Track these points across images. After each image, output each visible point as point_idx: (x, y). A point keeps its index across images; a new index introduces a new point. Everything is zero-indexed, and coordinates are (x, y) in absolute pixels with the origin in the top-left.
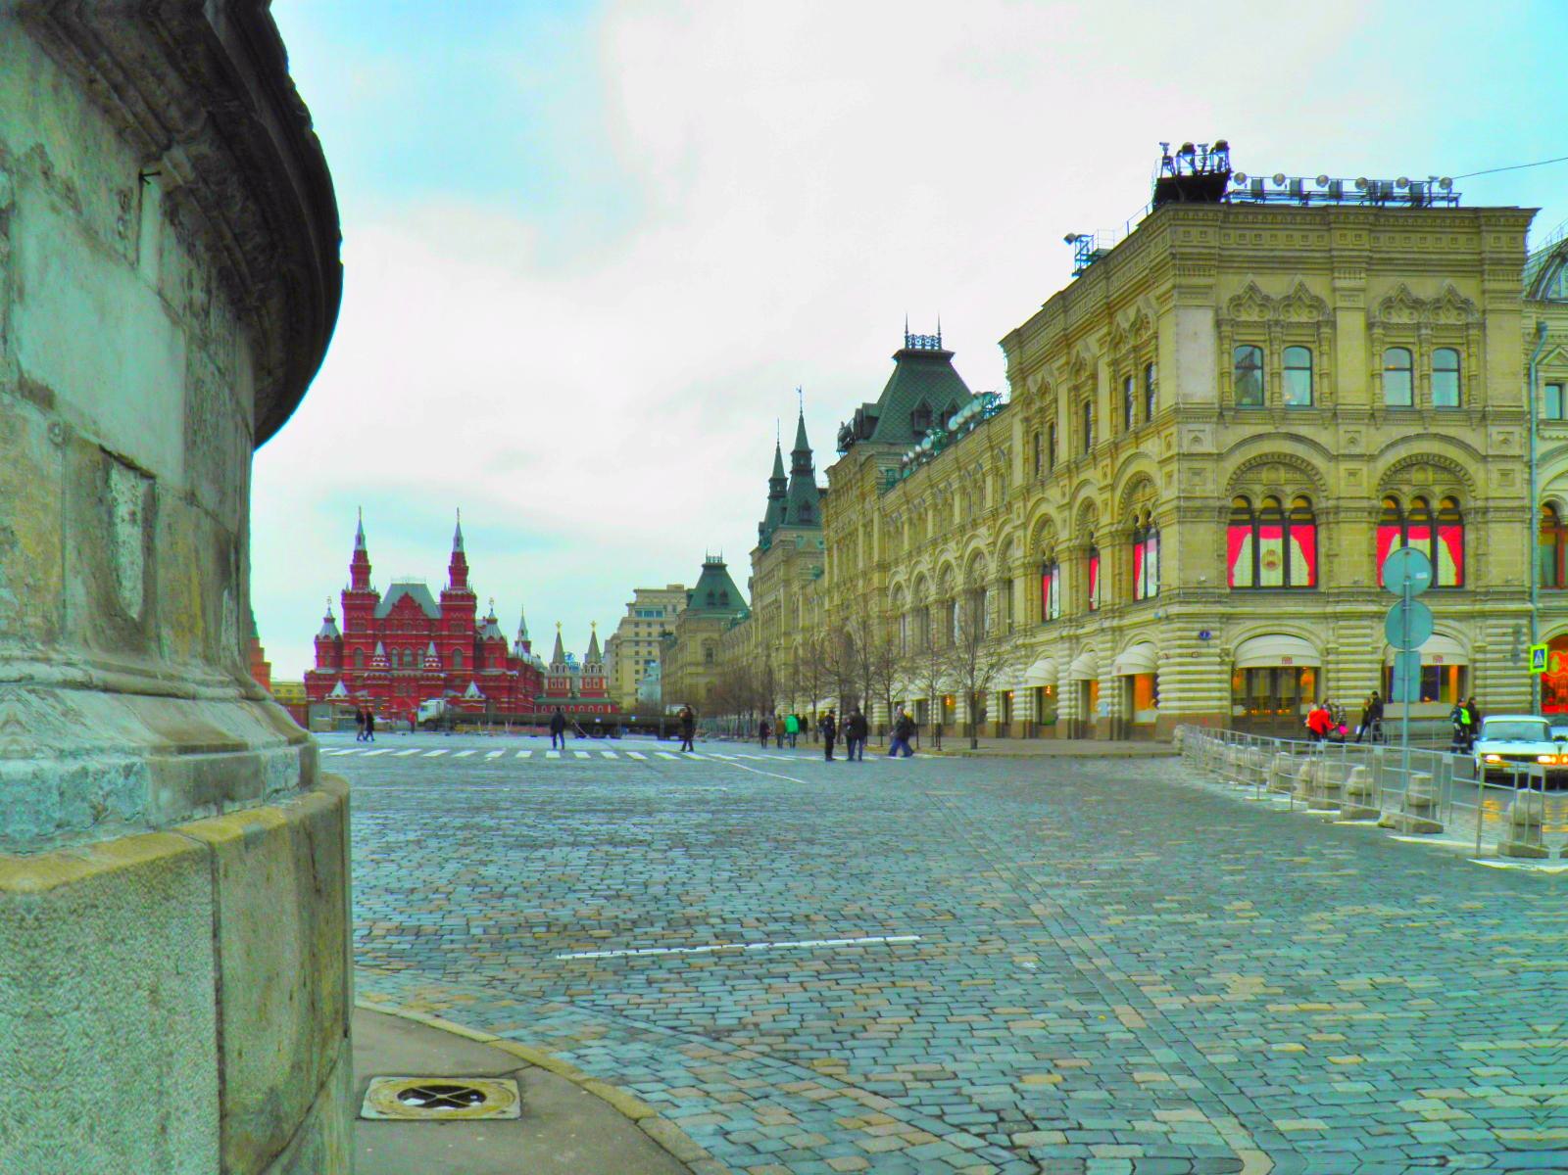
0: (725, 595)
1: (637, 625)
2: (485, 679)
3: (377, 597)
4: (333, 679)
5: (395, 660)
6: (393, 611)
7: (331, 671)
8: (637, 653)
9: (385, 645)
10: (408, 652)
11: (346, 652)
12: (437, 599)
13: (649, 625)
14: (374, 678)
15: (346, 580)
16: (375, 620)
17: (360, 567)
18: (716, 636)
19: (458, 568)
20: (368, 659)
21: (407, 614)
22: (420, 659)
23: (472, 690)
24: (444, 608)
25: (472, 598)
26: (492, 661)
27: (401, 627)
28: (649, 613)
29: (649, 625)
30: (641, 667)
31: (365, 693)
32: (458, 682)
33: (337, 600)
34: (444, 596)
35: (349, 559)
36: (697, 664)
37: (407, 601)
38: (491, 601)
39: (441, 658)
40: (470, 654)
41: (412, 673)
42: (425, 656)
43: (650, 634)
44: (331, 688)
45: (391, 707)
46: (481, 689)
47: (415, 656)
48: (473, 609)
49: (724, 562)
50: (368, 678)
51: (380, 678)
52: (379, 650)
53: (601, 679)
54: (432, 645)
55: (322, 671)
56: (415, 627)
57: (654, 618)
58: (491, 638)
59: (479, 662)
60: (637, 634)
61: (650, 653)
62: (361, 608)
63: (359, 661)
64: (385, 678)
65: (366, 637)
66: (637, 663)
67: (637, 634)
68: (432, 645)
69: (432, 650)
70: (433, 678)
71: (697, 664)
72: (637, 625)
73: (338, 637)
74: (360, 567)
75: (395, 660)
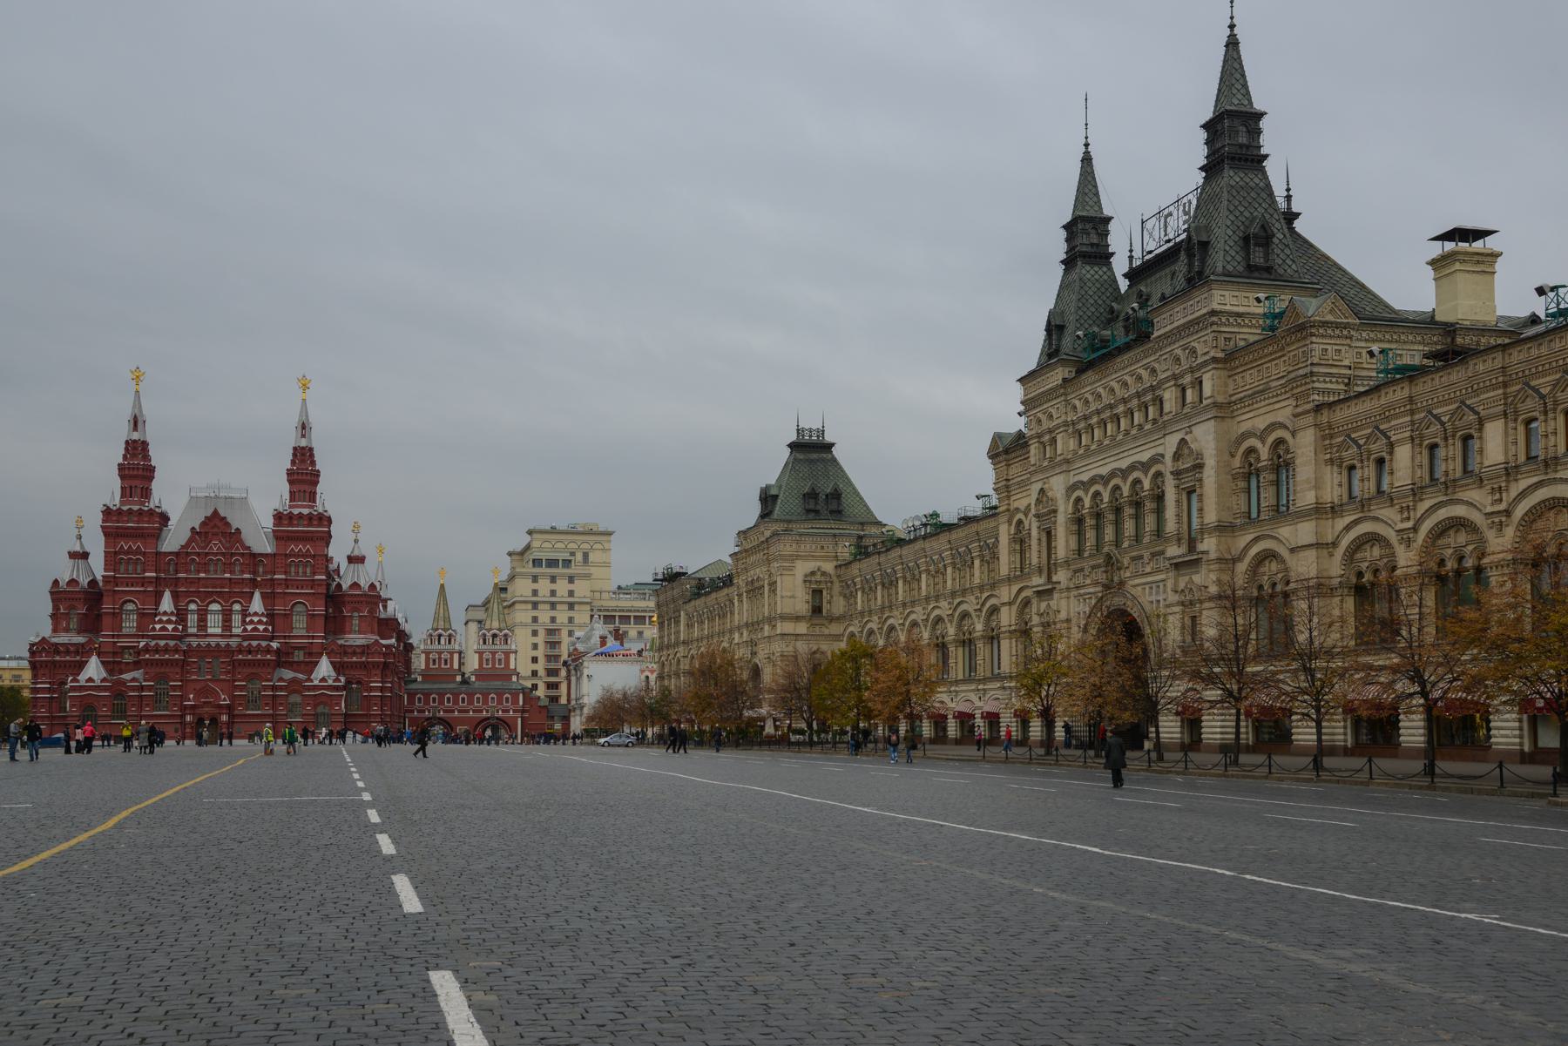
0: (836, 495)
1: (535, 579)
2: (344, 650)
3: (164, 519)
4: (83, 652)
5: (192, 619)
7: (81, 639)
8: (535, 619)
9: (176, 596)
10: (215, 607)
11: (107, 607)
12: (269, 522)
13: (553, 579)
14: (157, 650)
15: (110, 491)
16: (158, 554)
18: (829, 567)
19: (304, 473)
20: (147, 617)
21: (216, 546)
22: (236, 619)
23: (324, 669)
24: (279, 537)
26: (356, 622)
27: (204, 567)
28: (552, 563)
29: (553, 579)
30: (540, 639)
31: (138, 674)
32: (299, 656)
34: (279, 517)
36: (798, 618)
37: (216, 528)
38: (356, 528)
39: (271, 616)
40: (320, 610)
41: (223, 642)
42: (245, 613)
43: (553, 593)
44: (81, 666)
45: (183, 698)
46: (338, 668)
47: (227, 616)
48: (327, 538)
49: (828, 438)
50: (147, 649)
51: (166, 649)
52: (167, 604)
53: (507, 654)
54: (257, 596)
55: (63, 638)
56: (229, 567)
57: (560, 570)
58: (355, 585)
59: (334, 623)
60: (535, 593)
61: (553, 619)
62: (138, 534)
64: (176, 650)
65: (143, 582)
66: (535, 633)
67: (535, 593)
68: (257, 596)
69: (257, 605)
70: (258, 649)
71: (798, 618)
72: (535, 579)
73: (93, 582)
75: (192, 619)
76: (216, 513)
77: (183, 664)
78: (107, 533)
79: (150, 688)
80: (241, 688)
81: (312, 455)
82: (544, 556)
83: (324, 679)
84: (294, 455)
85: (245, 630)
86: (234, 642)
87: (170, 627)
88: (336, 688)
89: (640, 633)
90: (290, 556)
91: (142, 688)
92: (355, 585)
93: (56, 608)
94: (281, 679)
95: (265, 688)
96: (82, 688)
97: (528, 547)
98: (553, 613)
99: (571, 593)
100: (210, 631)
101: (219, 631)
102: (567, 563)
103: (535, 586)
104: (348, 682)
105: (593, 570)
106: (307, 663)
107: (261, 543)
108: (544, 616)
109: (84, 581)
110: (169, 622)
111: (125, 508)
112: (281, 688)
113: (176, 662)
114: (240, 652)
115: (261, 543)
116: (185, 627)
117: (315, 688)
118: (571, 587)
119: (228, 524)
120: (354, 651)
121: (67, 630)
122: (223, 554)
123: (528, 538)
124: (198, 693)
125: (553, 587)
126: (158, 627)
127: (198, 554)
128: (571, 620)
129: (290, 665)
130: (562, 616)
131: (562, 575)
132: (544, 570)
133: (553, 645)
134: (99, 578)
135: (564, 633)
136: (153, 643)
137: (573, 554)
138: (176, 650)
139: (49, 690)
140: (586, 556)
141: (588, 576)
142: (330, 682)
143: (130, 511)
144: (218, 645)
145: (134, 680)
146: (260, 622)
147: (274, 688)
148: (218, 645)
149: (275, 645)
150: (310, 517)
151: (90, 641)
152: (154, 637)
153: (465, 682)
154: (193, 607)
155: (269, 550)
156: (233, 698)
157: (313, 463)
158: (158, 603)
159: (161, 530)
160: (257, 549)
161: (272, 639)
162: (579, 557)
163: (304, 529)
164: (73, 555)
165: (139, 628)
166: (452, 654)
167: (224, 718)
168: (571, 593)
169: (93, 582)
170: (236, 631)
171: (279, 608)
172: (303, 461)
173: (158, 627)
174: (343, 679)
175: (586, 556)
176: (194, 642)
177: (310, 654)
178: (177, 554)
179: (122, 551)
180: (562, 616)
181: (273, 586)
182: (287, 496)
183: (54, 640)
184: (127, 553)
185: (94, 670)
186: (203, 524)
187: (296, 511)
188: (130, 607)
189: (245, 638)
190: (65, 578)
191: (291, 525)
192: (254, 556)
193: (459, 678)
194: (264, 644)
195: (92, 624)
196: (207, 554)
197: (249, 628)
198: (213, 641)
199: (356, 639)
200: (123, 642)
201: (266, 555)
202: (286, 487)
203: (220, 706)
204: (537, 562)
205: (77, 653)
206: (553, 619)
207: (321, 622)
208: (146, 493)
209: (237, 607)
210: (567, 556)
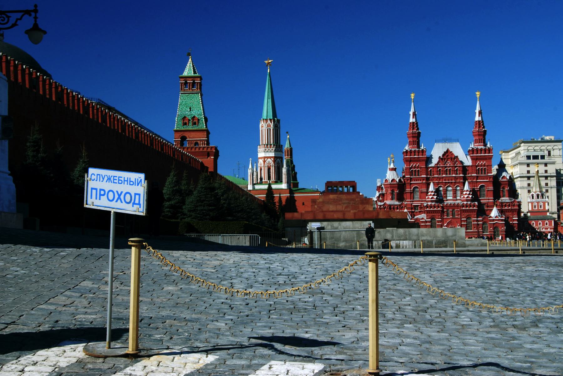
6: (439, 162)
8: (529, 185)
10: (450, 188)
21: (449, 163)
22: (459, 193)
28: (535, 157)
42: (462, 191)
47: (455, 192)
52: (431, 188)
59: (497, 195)
62: (418, 160)
63: (417, 196)
72: (528, 165)
76: (448, 150)
77: (443, 211)
82: (532, 154)
85: (464, 197)
99: (546, 171)
101: (451, 198)
102: (543, 157)
103: (528, 169)
117: (493, 220)
118: (546, 168)
121: (392, 199)
128: (547, 184)
140: (549, 154)
145: (423, 219)
155: (469, 165)
165: (420, 198)
173: (430, 197)
178: (433, 167)
186: (443, 155)
195: (400, 198)
196: (446, 167)
200: (415, 204)
207: (492, 193)
209: (458, 188)
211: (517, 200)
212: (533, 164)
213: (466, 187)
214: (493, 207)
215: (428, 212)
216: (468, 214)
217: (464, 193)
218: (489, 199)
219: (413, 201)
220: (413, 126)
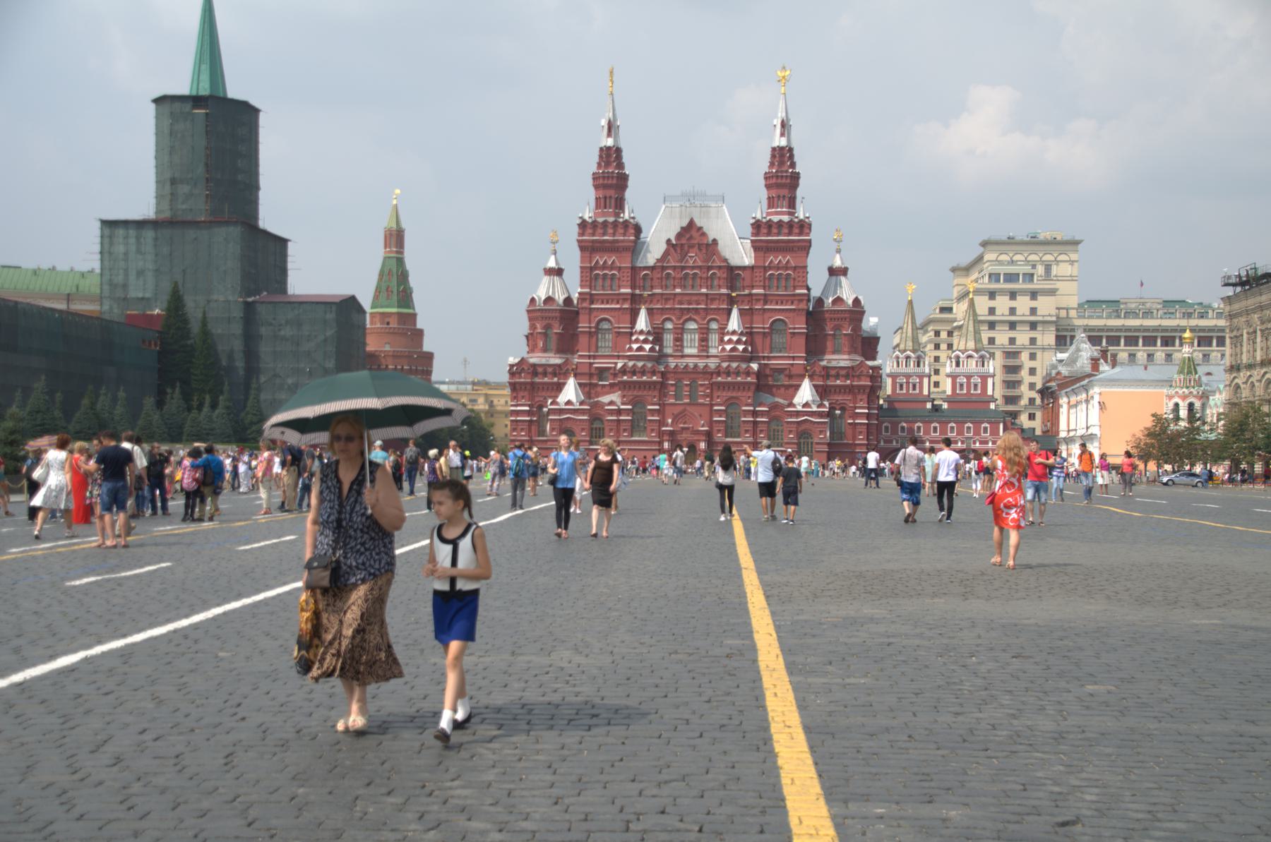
2: (827, 372)
4: (561, 372)
7: (557, 360)
10: (692, 326)
11: (583, 325)
13: (1013, 295)
14: (634, 372)
17: (611, 179)
19: (783, 177)
21: (694, 258)
22: (714, 338)
23: (805, 393)
24: (757, 247)
25: (804, 226)
28: (1011, 278)
29: (1013, 295)
31: (615, 397)
33: (571, 236)
35: (591, 164)
37: (691, 238)
39: (750, 334)
40: (801, 326)
41: (701, 363)
42: (722, 331)
43: (1013, 311)
44: (559, 387)
45: (662, 423)
46: (822, 392)
48: (806, 247)
50: (624, 371)
51: (643, 372)
52: (642, 323)
59: (815, 345)
61: (1012, 341)
62: (611, 248)
63: (606, 342)
65: (620, 298)
68: (735, 313)
69: (734, 323)
74: (611, 179)
75: (668, 339)
76: (691, 223)
77: (662, 386)
78: (584, 247)
79: (627, 412)
80: (719, 413)
81: (792, 156)
83: (806, 405)
84: (773, 156)
85: (724, 349)
86: (713, 363)
87: (647, 347)
88: (820, 415)
89: (1169, 356)
90: (770, 268)
91: (619, 412)
92: (839, 300)
93: (533, 327)
94: (760, 405)
95: (746, 413)
96: (561, 411)
97: (980, 259)
98: (1012, 334)
99: (1033, 311)
100: (688, 351)
101: (694, 351)
102: (1030, 277)
104: (832, 408)
105: (1058, 285)
106: (787, 387)
107: (740, 253)
108: (1002, 337)
109: (560, 297)
110: (645, 341)
111: (601, 220)
112: (762, 414)
113: (655, 381)
114: (719, 374)
115: (740, 253)
116: (661, 346)
117: (798, 414)
118: (1034, 304)
119: (704, 234)
120: (839, 372)
121: (545, 350)
122: (700, 268)
123: (982, 249)
124: (676, 419)
125: (1013, 304)
126: (635, 346)
127: (674, 268)
128: (1033, 341)
129: (769, 389)
130: (1023, 337)
131: (1023, 292)
132: (1002, 285)
133: (1013, 369)
134: (575, 296)
135: (1025, 356)
136: (631, 364)
137: (1034, 267)
138: (653, 373)
139: (528, 413)
141: (1052, 292)
142: (814, 409)
143: (605, 223)
144: (696, 366)
145: (611, 403)
146: (739, 342)
147: (755, 414)
148: (696, 366)
149: (755, 366)
150: (790, 225)
151: (566, 362)
152: (630, 358)
153: (936, 409)
154: (669, 325)
156: (711, 423)
157: (793, 165)
158: (633, 322)
159: (635, 242)
160: (735, 261)
161: (751, 359)
162: (1040, 270)
163: (783, 239)
164: (550, 272)
165: (614, 348)
166: (921, 377)
167: (703, 445)
168: (1033, 311)
169: (568, 301)
170: (713, 351)
171: (759, 326)
172: (782, 163)
173: (635, 346)
174: (826, 403)
175: (1048, 268)
176: (672, 363)
177: (790, 377)
178: (652, 268)
179: (596, 267)
180: (1023, 337)
181: (750, 302)
182: (765, 203)
183: (532, 361)
184: (604, 267)
185: (570, 392)
186: (679, 236)
187: (776, 219)
188: (605, 326)
189: (723, 359)
190: (541, 294)
191: (769, 234)
192: (731, 269)
193: (929, 406)
194: (744, 366)
195: (567, 344)
196: (683, 268)
197: (728, 347)
198: (691, 362)
199: (840, 360)
200: (599, 363)
201: (744, 268)
202: (764, 194)
203: (698, 433)
204: (994, 277)
205: (555, 375)
206: (1012, 341)
207: (802, 341)
208: (620, 204)
209: (714, 326)
210: (1028, 269)
211: (870, 363)
212: (1002, 292)
213: (734, 323)
214: (802, 377)
215: (624, 386)
216: (730, 394)
217: (726, 338)
218: (793, 358)
219: (595, 357)
220: (609, 156)
